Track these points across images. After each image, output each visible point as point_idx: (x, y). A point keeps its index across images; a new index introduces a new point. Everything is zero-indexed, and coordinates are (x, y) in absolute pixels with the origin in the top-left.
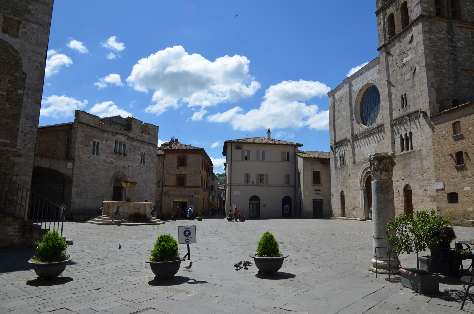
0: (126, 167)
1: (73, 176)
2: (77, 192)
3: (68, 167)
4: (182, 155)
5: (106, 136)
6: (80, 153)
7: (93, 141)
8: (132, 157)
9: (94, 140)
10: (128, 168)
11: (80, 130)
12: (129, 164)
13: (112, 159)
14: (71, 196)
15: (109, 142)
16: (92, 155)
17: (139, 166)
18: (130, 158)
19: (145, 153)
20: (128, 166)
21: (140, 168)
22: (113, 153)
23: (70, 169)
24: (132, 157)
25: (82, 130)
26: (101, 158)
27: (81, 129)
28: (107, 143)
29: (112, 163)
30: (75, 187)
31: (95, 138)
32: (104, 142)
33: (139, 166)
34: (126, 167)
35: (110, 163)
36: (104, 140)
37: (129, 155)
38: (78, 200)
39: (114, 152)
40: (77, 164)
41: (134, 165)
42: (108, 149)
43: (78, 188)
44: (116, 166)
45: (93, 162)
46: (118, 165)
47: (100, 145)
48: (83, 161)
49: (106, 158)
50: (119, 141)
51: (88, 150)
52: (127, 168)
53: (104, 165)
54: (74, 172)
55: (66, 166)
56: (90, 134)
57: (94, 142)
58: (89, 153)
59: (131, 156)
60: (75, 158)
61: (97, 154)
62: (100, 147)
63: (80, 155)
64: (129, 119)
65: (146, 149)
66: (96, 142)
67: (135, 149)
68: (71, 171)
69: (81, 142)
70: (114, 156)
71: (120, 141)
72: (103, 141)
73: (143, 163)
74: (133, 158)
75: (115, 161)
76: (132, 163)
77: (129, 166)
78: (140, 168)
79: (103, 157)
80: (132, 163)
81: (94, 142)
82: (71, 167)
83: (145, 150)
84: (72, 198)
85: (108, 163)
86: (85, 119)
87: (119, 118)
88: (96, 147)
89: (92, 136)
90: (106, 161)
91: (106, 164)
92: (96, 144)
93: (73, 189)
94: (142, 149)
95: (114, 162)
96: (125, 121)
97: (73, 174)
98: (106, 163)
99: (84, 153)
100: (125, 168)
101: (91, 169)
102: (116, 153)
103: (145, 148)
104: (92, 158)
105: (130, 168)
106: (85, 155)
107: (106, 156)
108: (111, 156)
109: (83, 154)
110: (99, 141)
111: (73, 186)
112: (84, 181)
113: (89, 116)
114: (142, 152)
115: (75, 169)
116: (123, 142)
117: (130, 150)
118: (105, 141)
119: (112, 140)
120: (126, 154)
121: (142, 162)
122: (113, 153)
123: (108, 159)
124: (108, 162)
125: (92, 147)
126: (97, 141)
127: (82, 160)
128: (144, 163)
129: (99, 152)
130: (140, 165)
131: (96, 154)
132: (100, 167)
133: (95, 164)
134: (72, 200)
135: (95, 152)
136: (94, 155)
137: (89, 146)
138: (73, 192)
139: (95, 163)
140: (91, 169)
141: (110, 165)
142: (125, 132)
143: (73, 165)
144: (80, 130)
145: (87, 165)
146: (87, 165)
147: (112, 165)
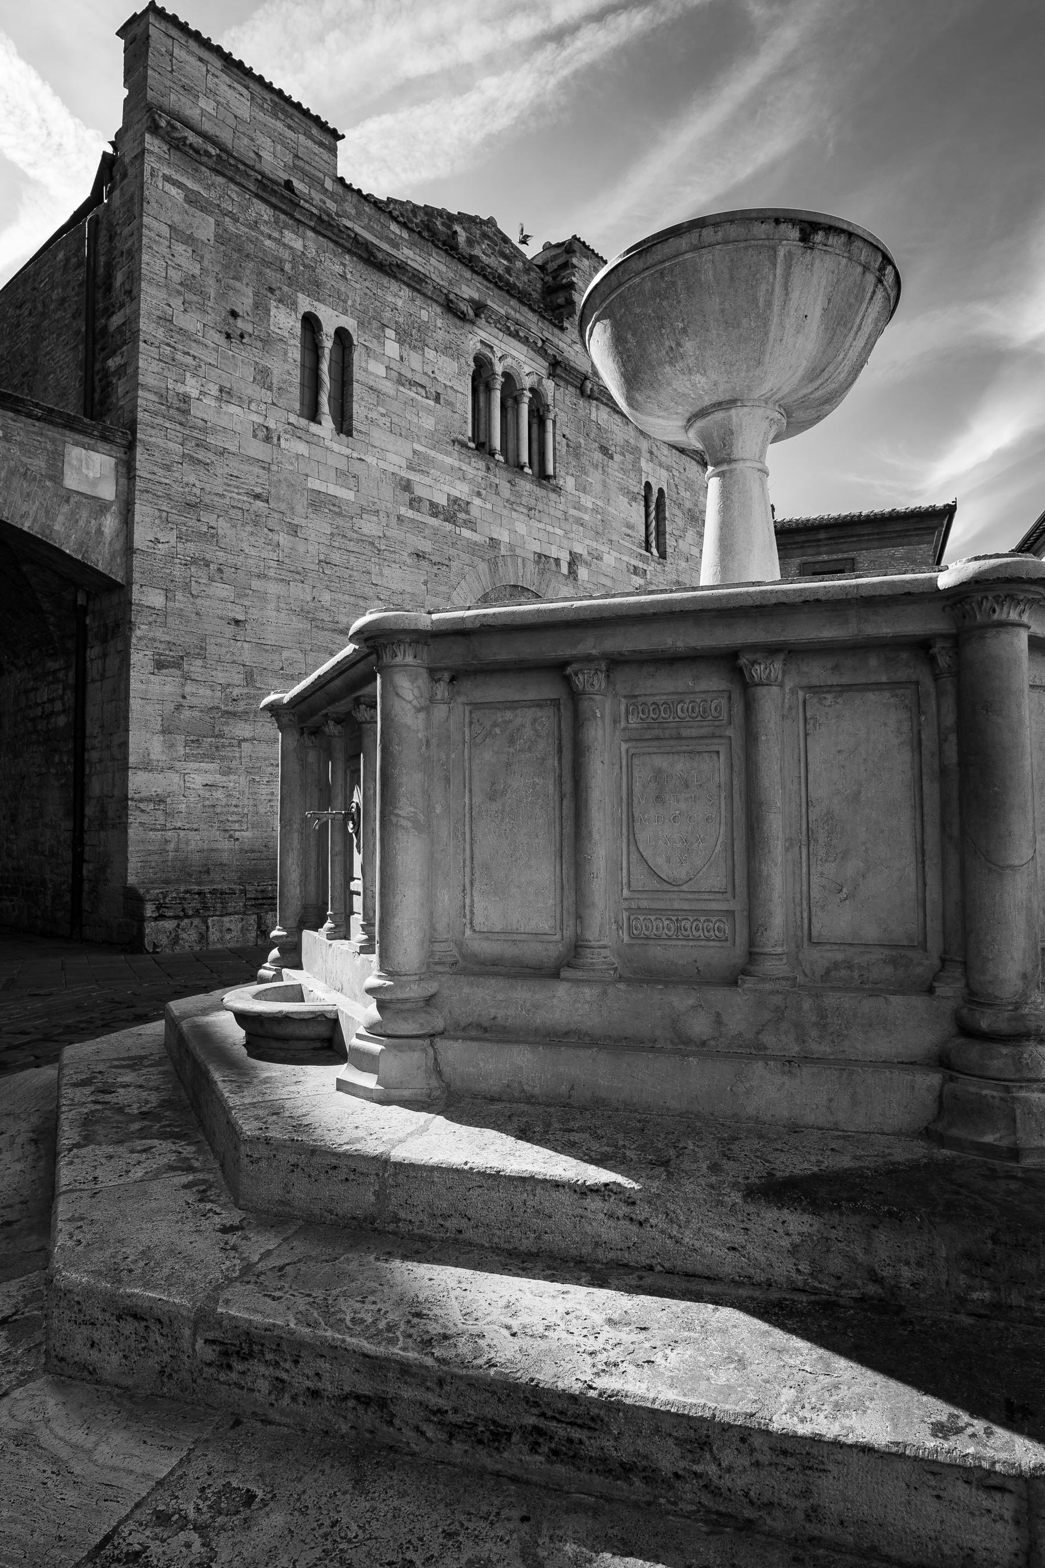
0: (557, 561)
1: (129, 570)
2: (179, 707)
3: (71, 481)
4: (825, 557)
5: (400, 303)
6: (190, 381)
7: (293, 306)
8: (587, 501)
9: (305, 304)
10: (572, 573)
11: (167, 179)
12: (579, 549)
13: (461, 490)
14: (125, 745)
15: (430, 354)
16: (293, 419)
17: (636, 571)
18: (578, 506)
19: (661, 491)
20: (568, 558)
21: (642, 582)
22: (463, 445)
23: (101, 507)
24: (587, 501)
25: (189, 184)
26: (369, 459)
27: (182, 179)
28: (415, 360)
29: (462, 516)
30: (160, 665)
31: (315, 288)
32: (392, 348)
33: (636, 571)
34: (557, 561)
35: (451, 519)
36: (390, 333)
37: (569, 483)
38: (198, 780)
39: (473, 439)
40: (168, 468)
41: (606, 556)
42: (430, 411)
43: (186, 677)
44: (494, 543)
45: (314, 484)
46: (504, 537)
47: (358, 356)
48: (223, 452)
49: (410, 468)
50: (499, 368)
51: (263, 376)
52: (565, 569)
53: (400, 518)
54: (141, 537)
55: (56, 476)
56: (268, 242)
57: (310, 322)
58: (267, 396)
59: (584, 490)
60: (141, 415)
61: (344, 425)
62: (357, 374)
63: (185, 399)
64: (555, 258)
65: (668, 469)
66: (329, 329)
67: (604, 450)
68: (110, 523)
69: (189, 284)
70: (474, 467)
71: (506, 374)
72: (380, 339)
73: (654, 551)
74: (595, 510)
75: (477, 501)
76: (594, 544)
77: (574, 560)
78: (642, 582)
79: (392, 457)
80: (594, 544)
81: (310, 322)
82: (108, 491)
83: (664, 473)
84: (132, 759)
85: (435, 510)
86: (207, 104)
87: (485, 236)
88: (325, 366)
89: (287, 267)
90: (419, 491)
91: (418, 517)
92: (328, 344)
93: (134, 685)
94: (643, 463)
95: (475, 512)
96: (527, 271)
97: (129, 550)
98: (415, 503)
99: (225, 394)
100: (553, 567)
101: (294, 530)
102: (481, 446)
103: (661, 465)
104: (301, 448)
105: (583, 573)
106: (232, 409)
107: (414, 452)
108: (448, 460)
109: (214, 390)
110: (349, 323)
111: (140, 659)
112: (237, 622)
113: (245, 92)
114: (648, 485)
115: (140, 510)
116: (528, 382)
117: (575, 451)
118: (400, 342)
119: (450, 350)
120: (550, 471)
121: (648, 548)
122: (463, 445)
123: (427, 480)
124: (432, 504)
125: (295, 353)
126: (330, 320)
127: (211, 439)
128: (663, 555)
129: (358, 410)
130: (641, 565)
131: (328, 423)
132: (369, 527)
133: (334, 502)
134: (138, 782)
135: (325, 408)
136: (314, 428)
137: (267, 342)
138: (135, 704)
139: (333, 490)
140: (294, 530)
141: (448, 527)
142: (535, 325)
143: (127, 470)
144: (167, 179)
145: (257, 497)
146: (257, 497)
147: (466, 533)
